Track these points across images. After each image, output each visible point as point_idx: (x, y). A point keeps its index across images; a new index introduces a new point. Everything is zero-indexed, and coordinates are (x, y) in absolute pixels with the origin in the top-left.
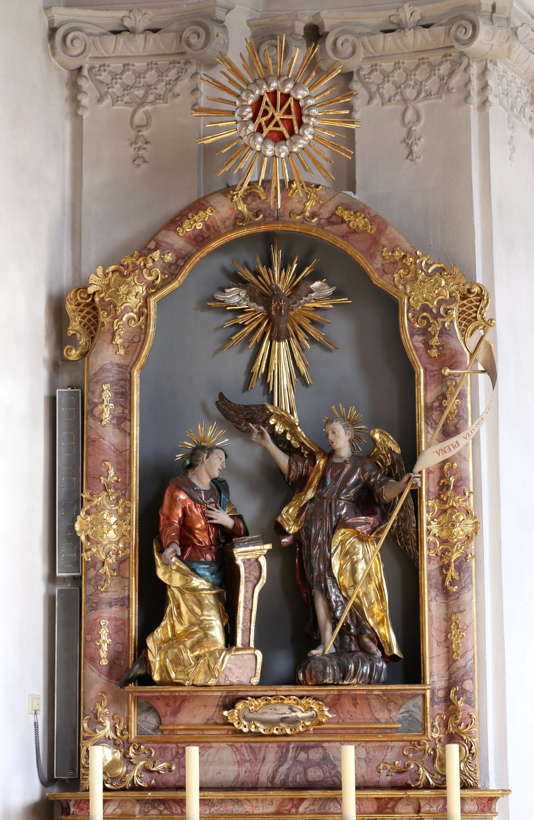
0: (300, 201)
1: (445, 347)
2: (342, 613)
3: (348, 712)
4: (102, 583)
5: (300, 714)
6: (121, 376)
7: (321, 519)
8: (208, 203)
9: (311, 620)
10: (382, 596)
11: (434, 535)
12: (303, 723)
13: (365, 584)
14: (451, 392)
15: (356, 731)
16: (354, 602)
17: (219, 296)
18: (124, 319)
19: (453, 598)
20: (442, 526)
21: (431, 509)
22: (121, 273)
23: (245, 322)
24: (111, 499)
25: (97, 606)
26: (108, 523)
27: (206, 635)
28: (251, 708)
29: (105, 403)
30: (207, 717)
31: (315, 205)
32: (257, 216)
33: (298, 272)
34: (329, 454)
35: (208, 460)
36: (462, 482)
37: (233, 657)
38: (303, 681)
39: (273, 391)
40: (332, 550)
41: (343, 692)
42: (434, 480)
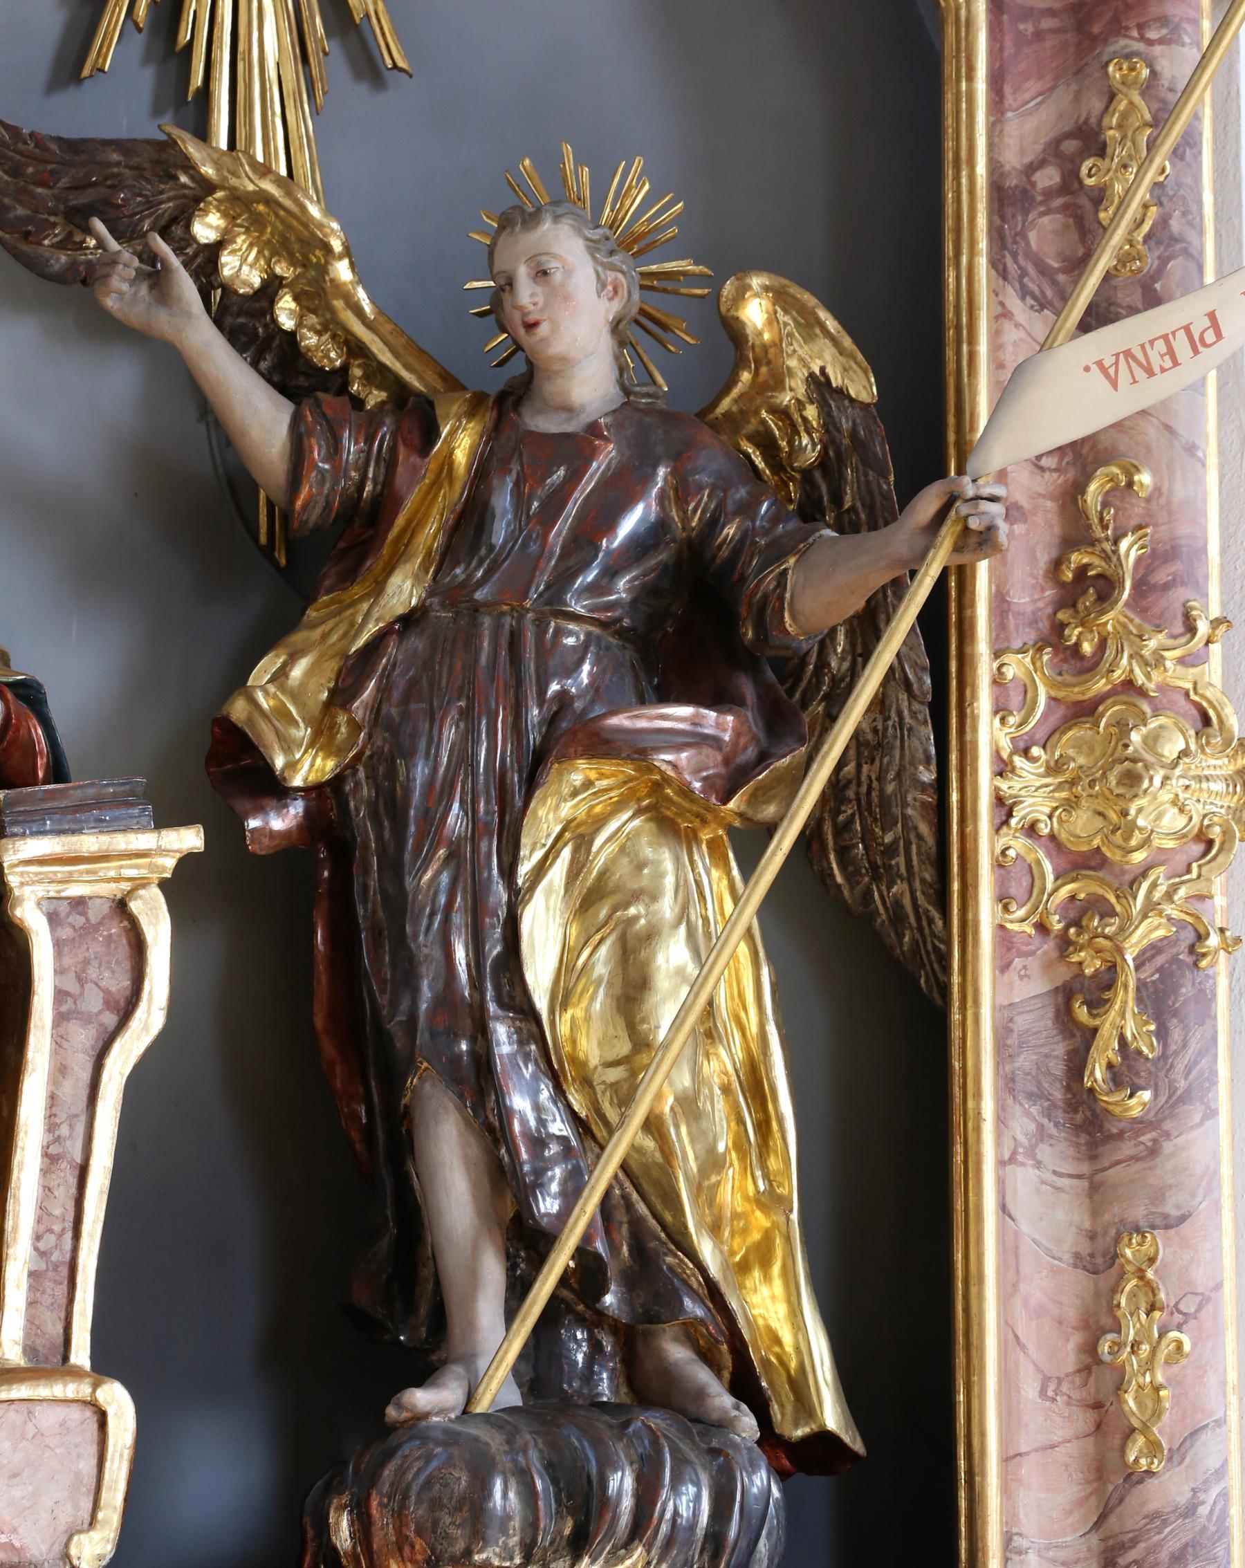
9: (385, 1243)
10: (763, 1127)
11: (1031, 829)
13: (688, 1052)
14: (1124, 116)
16: (633, 1147)
19: (1127, 1148)
20: (1073, 783)
21: (1015, 699)
34: (502, 398)
36: (1177, 567)
39: (205, 93)
40: (524, 869)
42: (1033, 551)
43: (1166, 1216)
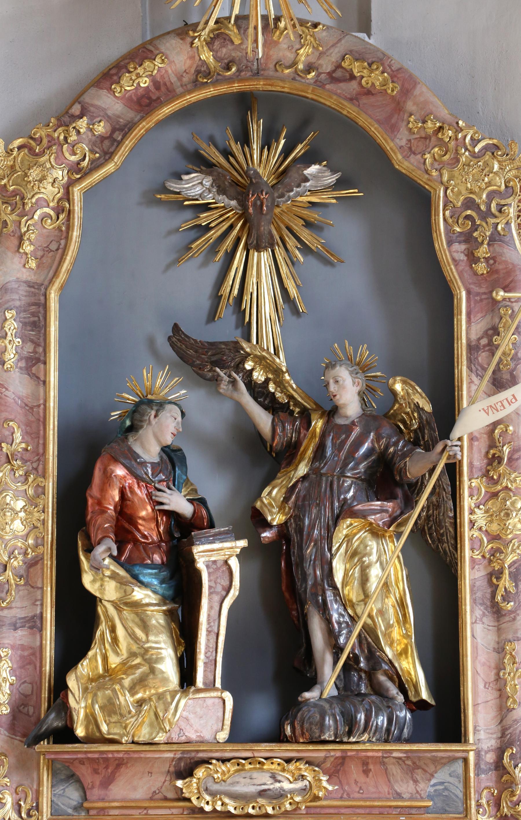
0: (290, 47)
1: (498, 259)
2: (348, 639)
3: (356, 782)
4: (3, 595)
5: (287, 786)
6: (33, 300)
7: (318, 505)
8: (157, 49)
9: (303, 650)
10: (405, 616)
11: (480, 529)
12: (292, 798)
13: (380, 598)
14: (505, 324)
15: (368, 811)
16: (365, 623)
17: (173, 186)
18: (36, 217)
19: (507, 619)
20: (492, 515)
21: (475, 492)
22: (31, 150)
23: (210, 223)
24: (17, 475)
26: (12, 509)
27: (152, 670)
28: (216, 776)
29: (9, 338)
30: (153, 789)
31: (313, 53)
32: (228, 69)
33: (287, 151)
34: (330, 412)
35: (157, 419)
37: (190, 702)
38: (291, 737)
39: (250, 323)
40: (334, 549)
41: (349, 754)
42: (480, 450)
43: (518, 637)
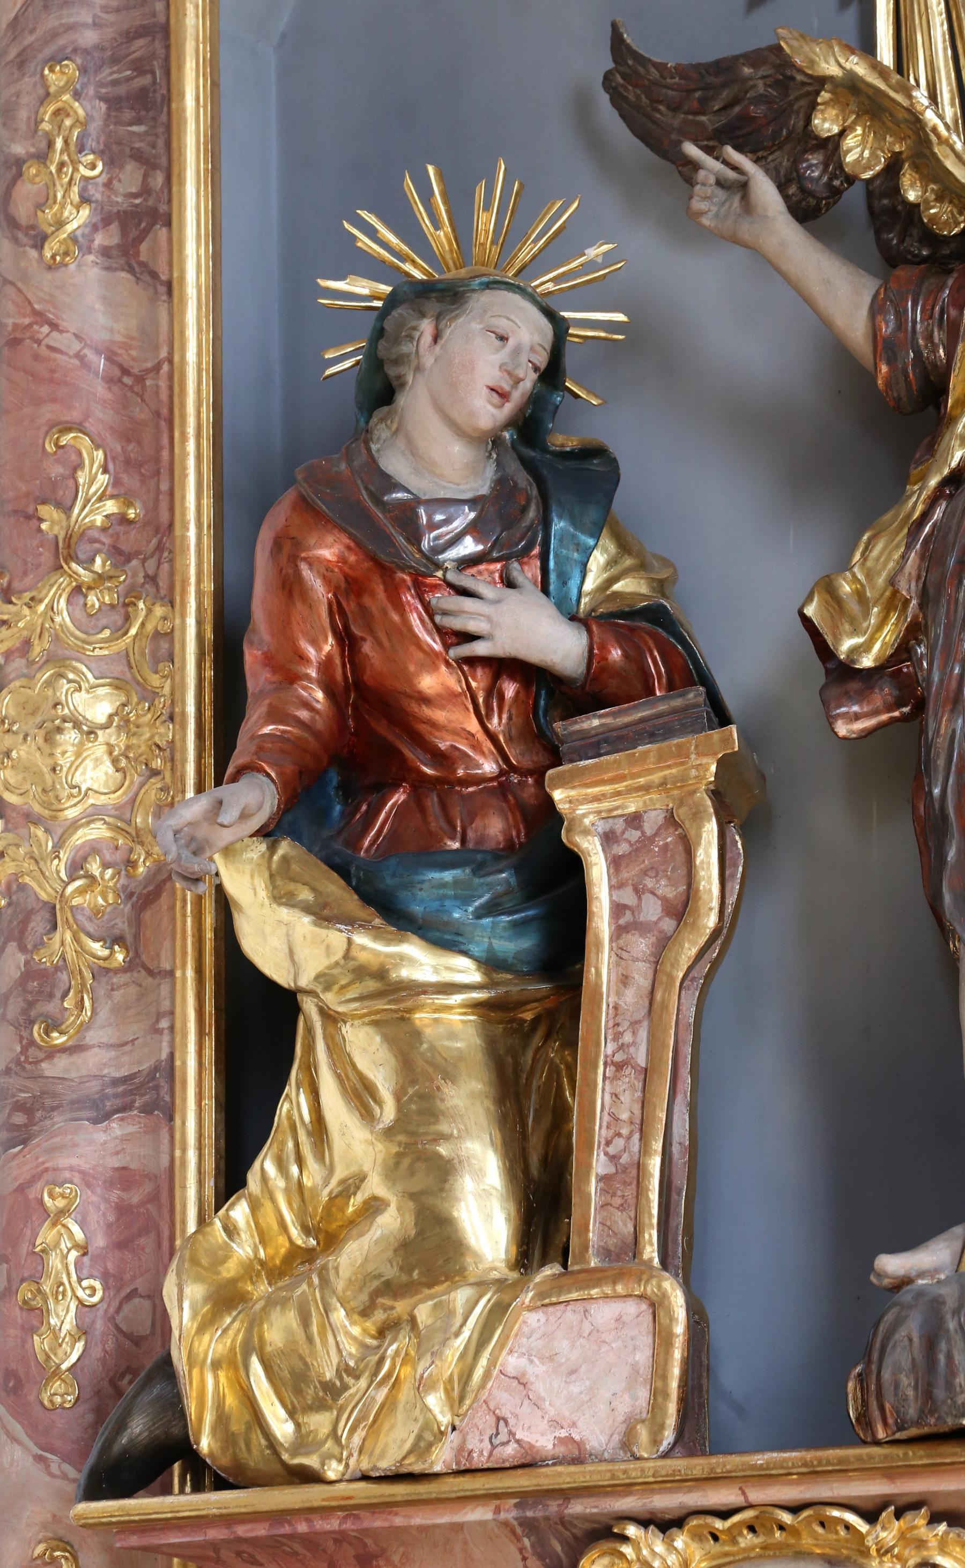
25: (31, 1122)
35: (437, 348)
